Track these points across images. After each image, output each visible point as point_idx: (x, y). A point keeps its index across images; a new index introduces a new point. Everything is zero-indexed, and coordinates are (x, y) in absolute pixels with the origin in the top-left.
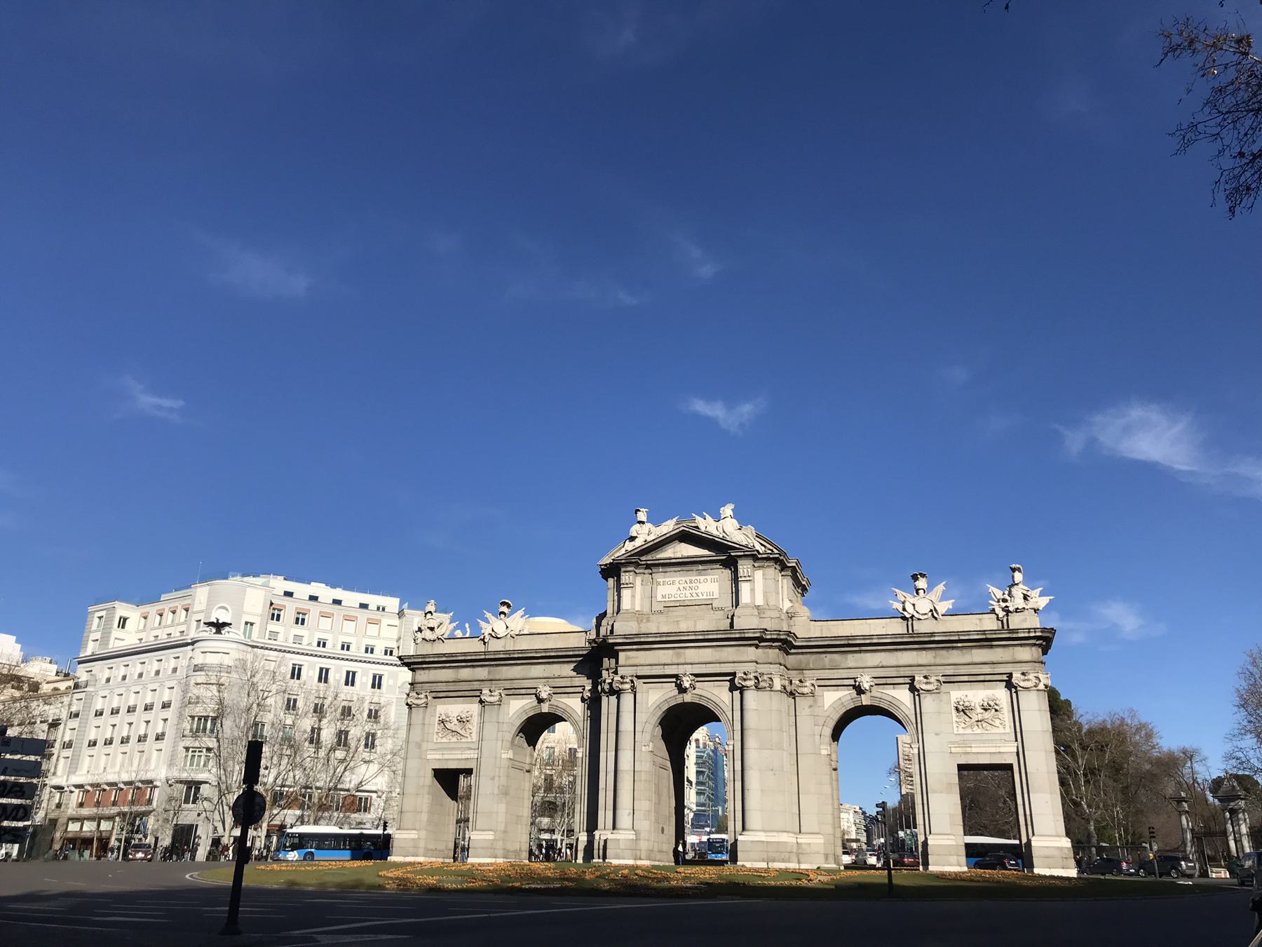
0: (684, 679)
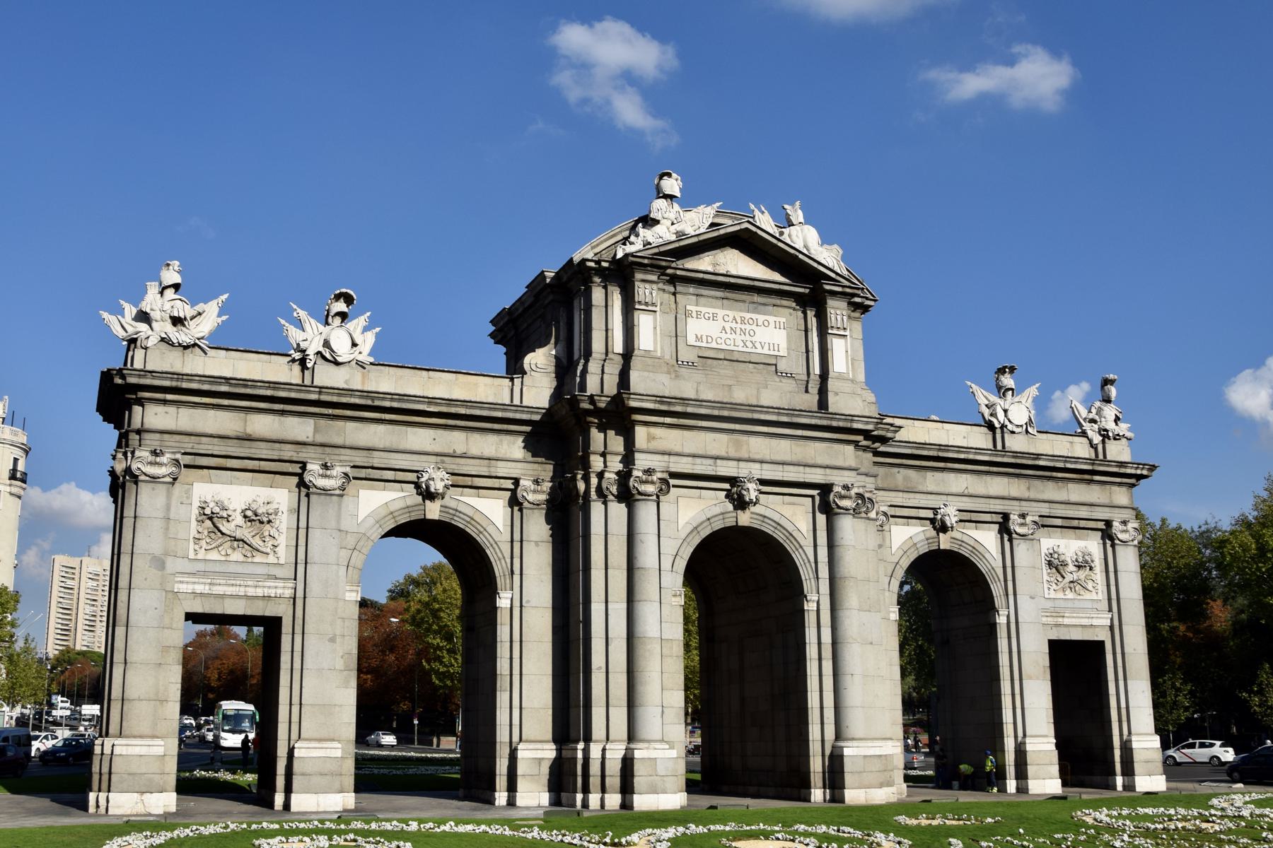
0: (752, 486)
